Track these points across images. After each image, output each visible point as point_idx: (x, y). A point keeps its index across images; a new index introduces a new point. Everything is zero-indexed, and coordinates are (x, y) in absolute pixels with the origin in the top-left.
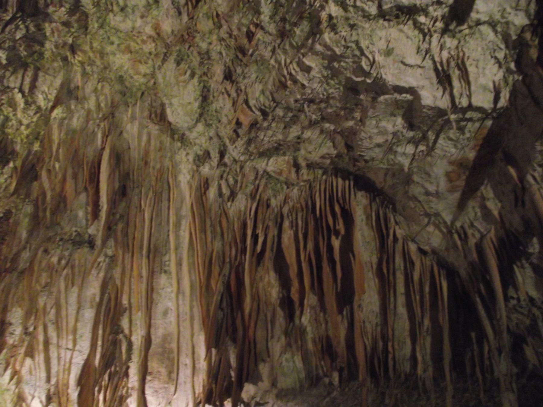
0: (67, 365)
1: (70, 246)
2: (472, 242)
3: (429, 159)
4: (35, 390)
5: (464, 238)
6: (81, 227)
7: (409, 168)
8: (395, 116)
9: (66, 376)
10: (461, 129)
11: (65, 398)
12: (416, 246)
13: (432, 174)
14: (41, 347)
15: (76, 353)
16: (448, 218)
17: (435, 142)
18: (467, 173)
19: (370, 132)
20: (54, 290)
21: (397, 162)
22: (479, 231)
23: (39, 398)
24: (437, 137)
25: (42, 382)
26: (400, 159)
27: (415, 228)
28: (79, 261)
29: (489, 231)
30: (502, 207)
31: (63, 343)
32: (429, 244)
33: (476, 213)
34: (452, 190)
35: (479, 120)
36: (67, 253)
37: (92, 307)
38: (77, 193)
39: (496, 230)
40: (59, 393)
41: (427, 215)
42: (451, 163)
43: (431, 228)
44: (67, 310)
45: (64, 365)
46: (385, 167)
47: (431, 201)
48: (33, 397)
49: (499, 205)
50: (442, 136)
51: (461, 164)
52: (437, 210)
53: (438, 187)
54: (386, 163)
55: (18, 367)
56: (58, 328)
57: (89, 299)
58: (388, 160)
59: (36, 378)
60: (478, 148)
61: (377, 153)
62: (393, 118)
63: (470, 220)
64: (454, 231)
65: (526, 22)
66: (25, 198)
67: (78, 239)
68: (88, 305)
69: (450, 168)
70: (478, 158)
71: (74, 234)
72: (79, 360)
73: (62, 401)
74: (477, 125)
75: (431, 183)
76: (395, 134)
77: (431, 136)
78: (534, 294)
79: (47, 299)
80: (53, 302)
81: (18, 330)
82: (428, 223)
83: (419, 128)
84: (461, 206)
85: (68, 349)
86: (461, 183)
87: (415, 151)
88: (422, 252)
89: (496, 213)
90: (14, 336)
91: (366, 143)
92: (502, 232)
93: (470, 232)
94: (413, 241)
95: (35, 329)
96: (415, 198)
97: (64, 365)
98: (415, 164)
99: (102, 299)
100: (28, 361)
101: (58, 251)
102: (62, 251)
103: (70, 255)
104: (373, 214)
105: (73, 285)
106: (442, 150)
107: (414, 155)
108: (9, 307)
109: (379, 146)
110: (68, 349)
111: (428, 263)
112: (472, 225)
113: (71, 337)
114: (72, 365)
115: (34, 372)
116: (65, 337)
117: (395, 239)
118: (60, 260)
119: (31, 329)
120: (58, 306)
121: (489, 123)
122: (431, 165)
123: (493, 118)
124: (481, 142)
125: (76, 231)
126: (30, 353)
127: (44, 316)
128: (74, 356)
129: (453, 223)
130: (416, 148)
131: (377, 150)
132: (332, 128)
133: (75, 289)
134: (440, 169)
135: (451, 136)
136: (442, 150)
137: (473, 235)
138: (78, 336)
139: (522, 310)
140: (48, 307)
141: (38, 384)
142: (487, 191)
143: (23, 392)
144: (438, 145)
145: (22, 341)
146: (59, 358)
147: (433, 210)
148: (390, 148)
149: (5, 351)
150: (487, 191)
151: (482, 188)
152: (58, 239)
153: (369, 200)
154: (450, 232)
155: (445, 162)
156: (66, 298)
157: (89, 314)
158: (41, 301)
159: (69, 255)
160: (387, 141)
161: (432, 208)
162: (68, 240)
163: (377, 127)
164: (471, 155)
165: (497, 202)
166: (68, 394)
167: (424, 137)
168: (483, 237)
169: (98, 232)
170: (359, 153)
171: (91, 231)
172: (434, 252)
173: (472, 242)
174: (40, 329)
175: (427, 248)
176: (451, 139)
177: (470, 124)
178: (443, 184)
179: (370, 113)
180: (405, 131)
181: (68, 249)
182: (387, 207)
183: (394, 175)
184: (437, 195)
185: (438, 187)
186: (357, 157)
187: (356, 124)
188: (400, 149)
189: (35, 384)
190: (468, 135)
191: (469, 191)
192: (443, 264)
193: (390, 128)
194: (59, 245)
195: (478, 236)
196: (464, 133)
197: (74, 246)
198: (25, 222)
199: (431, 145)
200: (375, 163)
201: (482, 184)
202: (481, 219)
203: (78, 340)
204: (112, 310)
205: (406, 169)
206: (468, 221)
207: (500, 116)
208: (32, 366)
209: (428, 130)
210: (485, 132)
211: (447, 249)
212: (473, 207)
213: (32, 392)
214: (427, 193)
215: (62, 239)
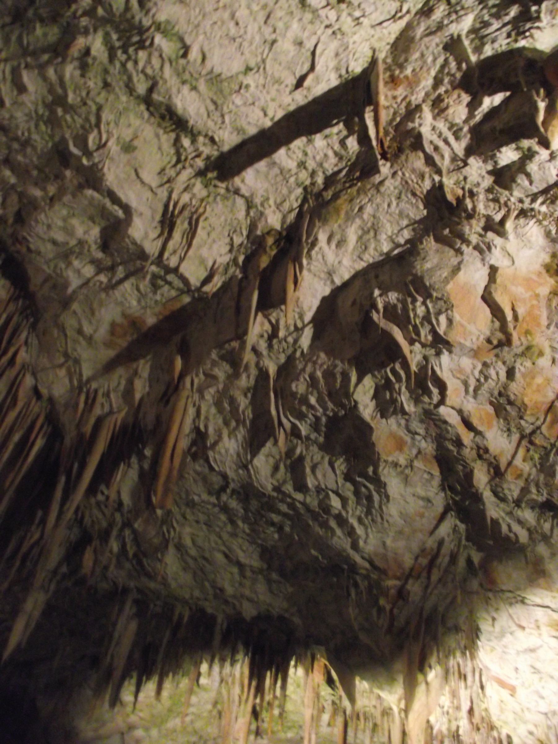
2: (97, 411)
3: (103, 295)
5: (90, 404)
7: (74, 292)
8: (94, 222)
10: (155, 287)
12: (34, 382)
13: (97, 313)
16: (87, 372)
17: (121, 281)
18: (135, 336)
19: (52, 219)
21: (65, 274)
22: (111, 405)
24: (126, 278)
26: (70, 274)
27: (44, 361)
29: (119, 411)
30: (148, 393)
32: (49, 388)
33: (119, 383)
34: (108, 345)
35: (178, 289)
39: (127, 414)
41: (66, 355)
42: (124, 315)
43: (62, 373)
46: (48, 271)
47: (79, 343)
49: (147, 389)
50: (132, 280)
51: (134, 323)
52: (80, 356)
53: (95, 331)
54: (52, 267)
58: (56, 266)
60: (161, 317)
61: (48, 250)
62: (91, 223)
63: (109, 386)
64: (85, 390)
65: (278, 227)
69: (119, 320)
70: (156, 328)
74: (173, 293)
75: (90, 322)
76: (81, 243)
77: (120, 272)
78: (126, 499)
82: (61, 366)
83: (112, 255)
84: (109, 367)
86: (123, 343)
87: (93, 277)
88: (36, 392)
89: (138, 396)
91: (40, 229)
92: (131, 420)
93: (100, 399)
94: (34, 374)
96: (63, 329)
98: (84, 291)
104: (4, 316)
106: (123, 296)
107: (88, 281)
109: (54, 242)
111: (36, 409)
112: (107, 395)
117: (12, 362)
121: (187, 299)
122: (101, 304)
123: (193, 297)
124: (167, 313)
129: (89, 381)
130: (97, 274)
131: (49, 246)
132: (13, 180)
134: (109, 314)
135: (142, 287)
136: (123, 296)
137: (102, 405)
139: (106, 511)
142: (144, 367)
144: (121, 287)
147: (75, 353)
148: (66, 255)
150: (144, 367)
151: (142, 362)
153: (9, 296)
154: (80, 388)
155: (119, 309)
160: (67, 243)
161: (76, 350)
163: (65, 220)
164: (151, 321)
165: (147, 385)
167: (112, 269)
168: (111, 412)
170: (25, 234)
172: (51, 400)
173: (97, 411)
175: (44, 391)
176: (138, 290)
177: (166, 287)
178: (102, 332)
179: (67, 198)
180: (94, 247)
182: (27, 317)
183: (54, 287)
184: (90, 340)
185: (95, 331)
186: (20, 238)
187: (43, 199)
188: (76, 263)
190: (158, 297)
191: (126, 357)
192: (52, 419)
193: (80, 231)
195: (107, 409)
196: (155, 293)
199: (114, 281)
200: (38, 258)
201: (144, 357)
202: (120, 394)
205: (70, 290)
206: (106, 386)
207: (200, 300)
209: (121, 264)
210: (178, 305)
211: (66, 406)
212: (120, 377)
214: (80, 332)
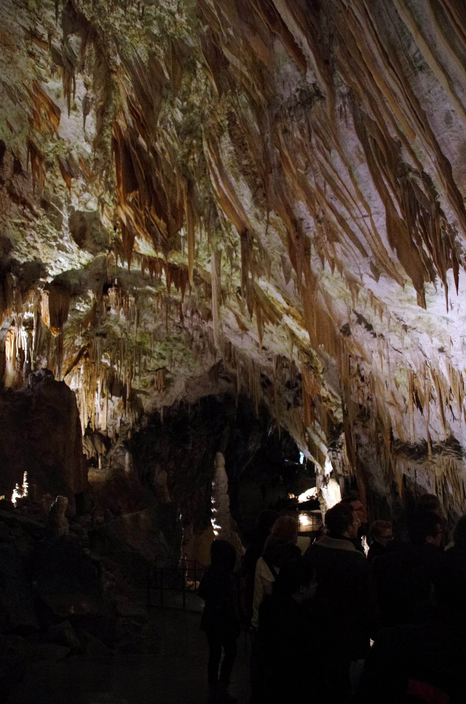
0: (373, 232)
1: (301, 111)
4: (359, 268)
6: (299, 82)
9: (378, 243)
11: (391, 264)
14: (340, 228)
15: (374, 217)
20: (316, 165)
23: (367, 274)
25: (362, 259)
28: (320, 120)
31: (356, 212)
36: (303, 121)
37: (362, 161)
38: (271, 47)
40: (380, 261)
44: (340, 179)
45: (370, 234)
48: (361, 275)
55: (332, 256)
56: (344, 202)
57: (354, 155)
59: (353, 257)
66: (233, 90)
67: (305, 98)
68: (357, 161)
71: (297, 94)
72: (381, 222)
73: (388, 268)
79: (315, 178)
80: (323, 178)
81: (311, 221)
85: (365, 216)
90: (311, 229)
95: (324, 213)
97: (370, 234)
99: (367, 148)
100: (337, 246)
101: (295, 124)
102: (298, 121)
103: (307, 120)
105: (330, 151)
108: (291, 205)
110: (365, 216)
113: (360, 204)
114: (378, 230)
115: (348, 253)
116: (354, 206)
118: (301, 131)
119: (321, 215)
120: (329, 179)
125: (297, 90)
126: (334, 238)
127: (324, 197)
128: (375, 220)
133: (335, 154)
138: (366, 199)
140: (321, 185)
141: (358, 262)
143: (349, 274)
145: (321, 230)
146: (362, 230)
149: (312, 246)
152: (287, 111)
156: (331, 166)
157: (363, 171)
158: (312, 184)
159: (306, 121)
162: (297, 105)
166: (390, 259)
169: (316, 77)
171: (310, 80)
174: (328, 211)
181: (301, 116)
189: (356, 264)
194: (292, 117)
197: (305, 108)
198: (250, 114)
203: (369, 203)
204: (384, 153)
208: (344, 248)
213: (357, 271)
215: (290, 109)
